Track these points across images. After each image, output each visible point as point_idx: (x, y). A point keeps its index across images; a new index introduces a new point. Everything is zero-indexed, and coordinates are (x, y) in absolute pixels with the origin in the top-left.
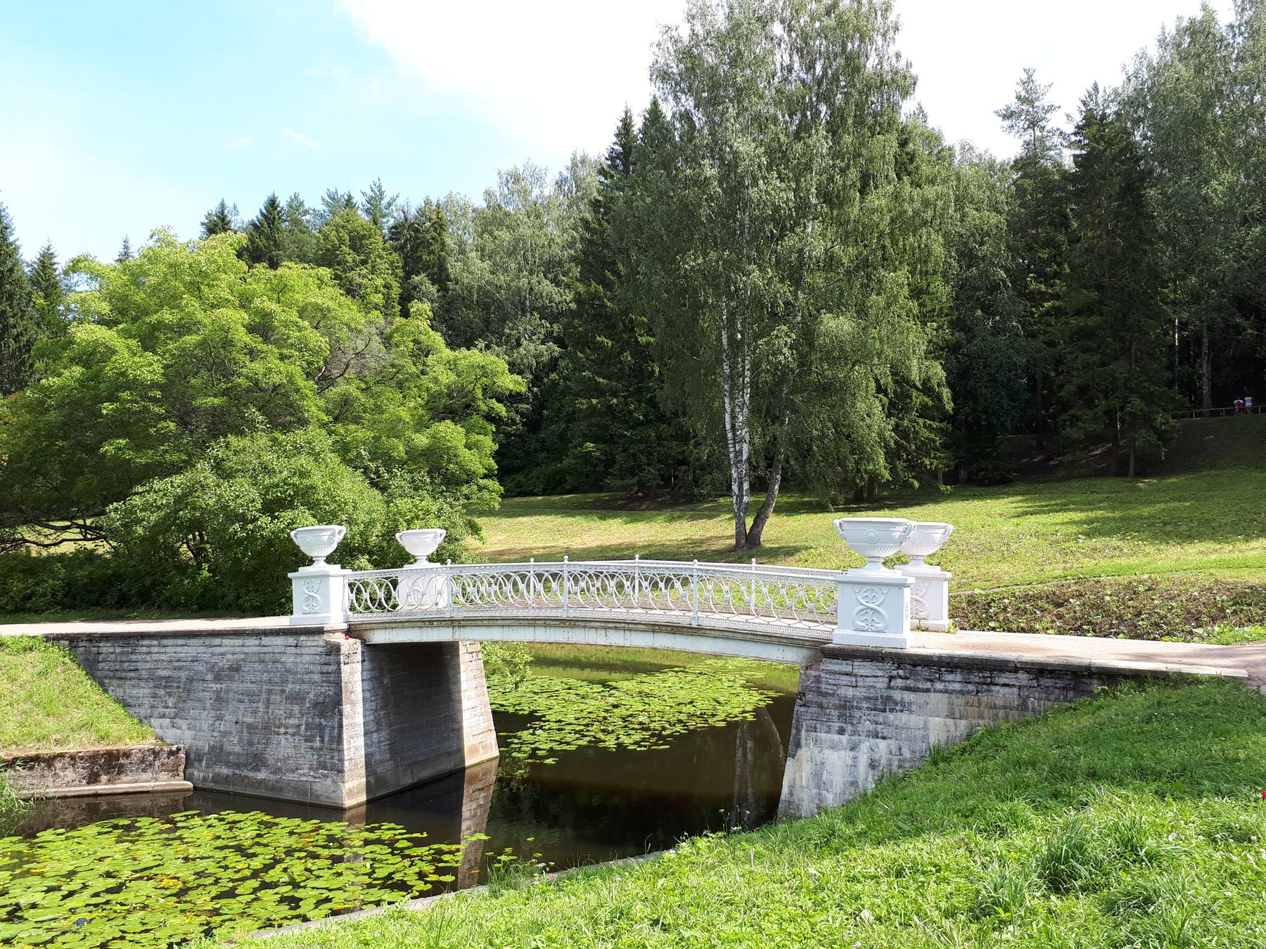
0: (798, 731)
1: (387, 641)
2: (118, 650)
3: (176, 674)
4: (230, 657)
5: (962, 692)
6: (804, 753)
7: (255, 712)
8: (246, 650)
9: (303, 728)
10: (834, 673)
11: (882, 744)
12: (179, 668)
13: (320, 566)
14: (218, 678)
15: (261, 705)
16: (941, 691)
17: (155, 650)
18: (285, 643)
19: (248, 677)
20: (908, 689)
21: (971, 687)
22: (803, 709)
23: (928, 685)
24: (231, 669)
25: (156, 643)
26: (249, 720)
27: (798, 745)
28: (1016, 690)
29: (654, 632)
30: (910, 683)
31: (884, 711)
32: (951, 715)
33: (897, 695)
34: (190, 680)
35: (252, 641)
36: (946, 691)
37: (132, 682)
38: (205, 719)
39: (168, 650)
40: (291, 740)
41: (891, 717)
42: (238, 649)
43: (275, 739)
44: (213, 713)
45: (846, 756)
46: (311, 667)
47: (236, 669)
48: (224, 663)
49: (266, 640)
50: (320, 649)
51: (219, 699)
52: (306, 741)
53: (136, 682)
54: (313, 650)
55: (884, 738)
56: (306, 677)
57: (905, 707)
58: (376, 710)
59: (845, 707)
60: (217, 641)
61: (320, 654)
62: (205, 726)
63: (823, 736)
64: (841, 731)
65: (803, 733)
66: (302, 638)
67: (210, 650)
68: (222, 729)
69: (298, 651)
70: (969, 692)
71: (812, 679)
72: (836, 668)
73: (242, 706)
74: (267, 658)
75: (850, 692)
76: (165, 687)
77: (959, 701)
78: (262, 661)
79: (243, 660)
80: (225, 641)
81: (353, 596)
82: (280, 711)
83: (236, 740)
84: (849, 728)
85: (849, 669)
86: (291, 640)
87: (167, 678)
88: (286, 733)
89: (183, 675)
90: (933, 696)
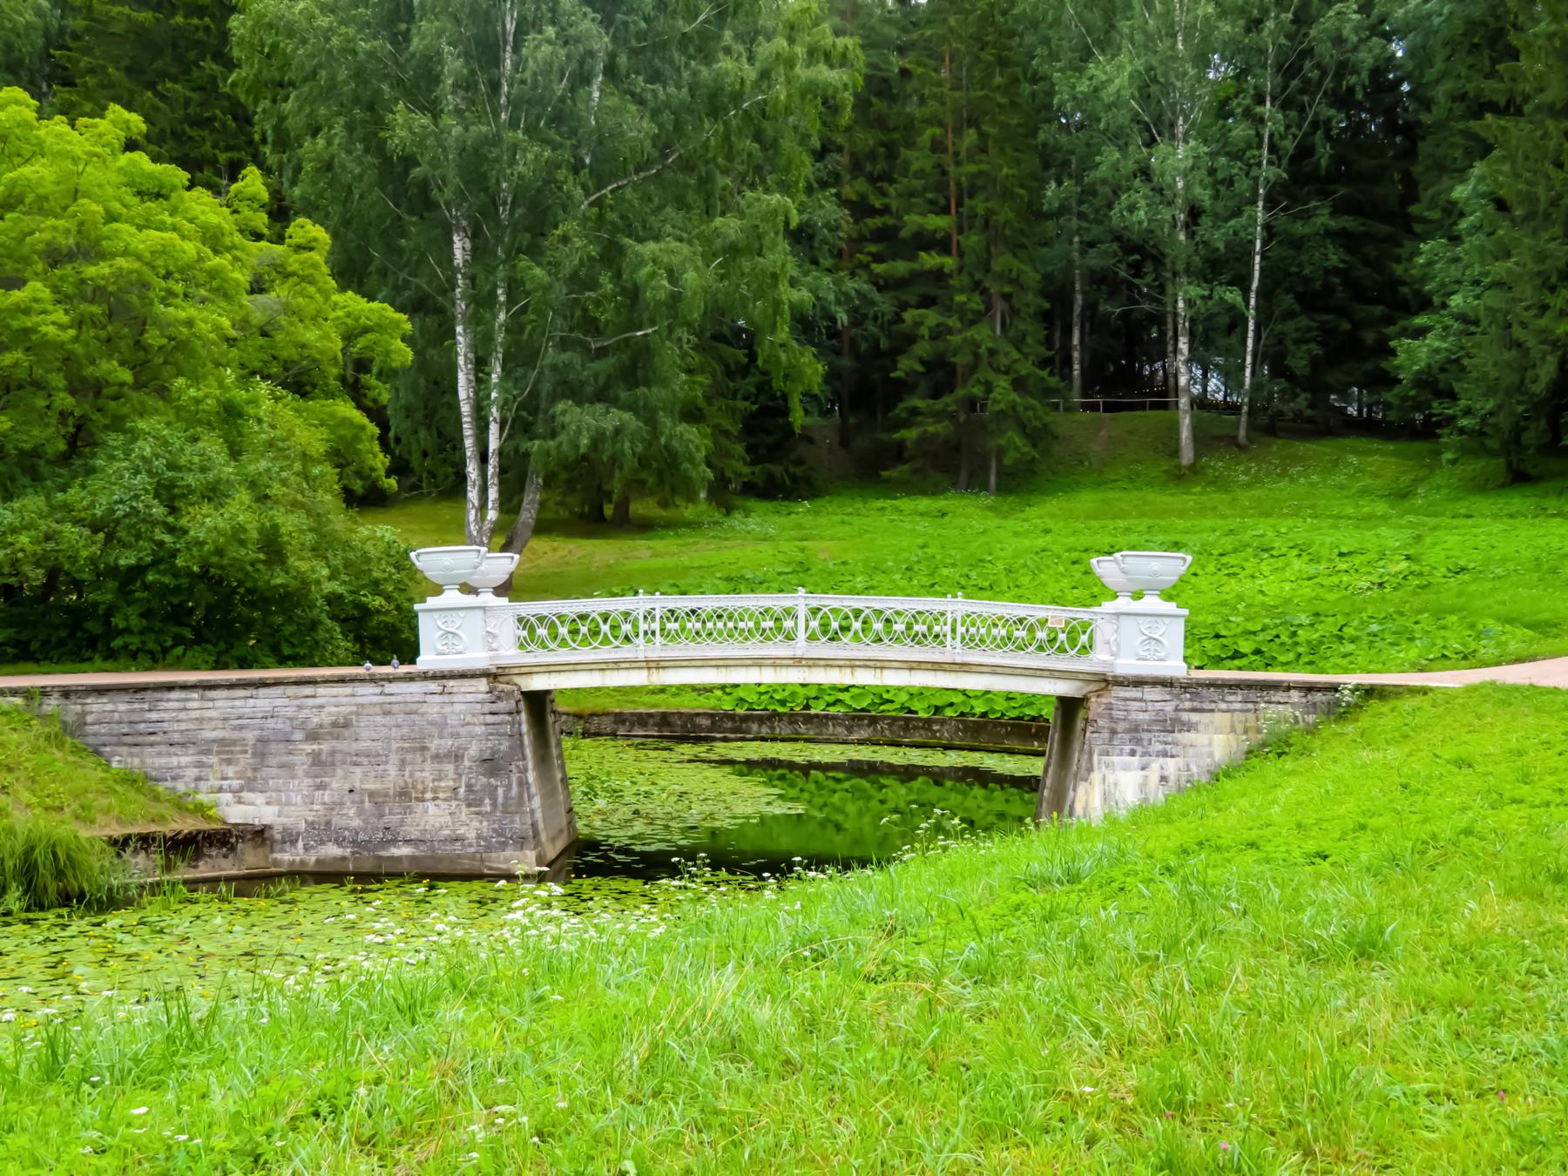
0: (1091, 754)
2: (123, 707)
3: (236, 735)
4: (335, 709)
5: (1242, 711)
6: (1096, 776)
7: (381, 777)
9: (462, 790)
10: (1126, 699)
12: (242, 728)
14: (313, 736)
17: (195, 705)
18: (424, 689)
19: (365, 734)
20: (1194, 710)
21: (1250, 706)
23: (1213, 706)
24: (334, 725)
25: (195, 695)
26: (371, 786)
27: (1090, 769)
29: (911, 669)
30: (1196, 704)
32: (1233, 730)
33: (1185, 716)
34: (263, 741)
35: (370, 689)
37: (156, 749)
38: (300, 786)
39: (219, 704)
40: (444, 805)
41: (1178, 736)
42: (344, 700)
45: (1135, 776)
46: (469, 718)
47: (342, 726)
48: (326, 718)
49: (390, 688)
50: (481, 697)
52: (469, 805)
53: (163, 748)
54: (470, 698)
56: (463, 731)
57: (1190, 727)
59: (1135, 729)
60: (308, 690)
63: (1115, 759)
64: (1133, 753)
65: (1095, 758)
66: (451, 683)
68: (326, 799)
69: (445, 698)
72: (1127, 695)
73: (358, 771)
74: (395, 708)
75: (1142, 716)
76: (219, 753)
77: (1239, 716)
78: (387, 713)
79: (358, 714)
80: (321, 690)
82: (425, 773)
83: (352, 812)
84: (1139, 750)
85: (1139, 695)
86: (433, 686)
87: (221, 742)
88: (434, 799)
89: (251, 736)
90: (1217, 716)
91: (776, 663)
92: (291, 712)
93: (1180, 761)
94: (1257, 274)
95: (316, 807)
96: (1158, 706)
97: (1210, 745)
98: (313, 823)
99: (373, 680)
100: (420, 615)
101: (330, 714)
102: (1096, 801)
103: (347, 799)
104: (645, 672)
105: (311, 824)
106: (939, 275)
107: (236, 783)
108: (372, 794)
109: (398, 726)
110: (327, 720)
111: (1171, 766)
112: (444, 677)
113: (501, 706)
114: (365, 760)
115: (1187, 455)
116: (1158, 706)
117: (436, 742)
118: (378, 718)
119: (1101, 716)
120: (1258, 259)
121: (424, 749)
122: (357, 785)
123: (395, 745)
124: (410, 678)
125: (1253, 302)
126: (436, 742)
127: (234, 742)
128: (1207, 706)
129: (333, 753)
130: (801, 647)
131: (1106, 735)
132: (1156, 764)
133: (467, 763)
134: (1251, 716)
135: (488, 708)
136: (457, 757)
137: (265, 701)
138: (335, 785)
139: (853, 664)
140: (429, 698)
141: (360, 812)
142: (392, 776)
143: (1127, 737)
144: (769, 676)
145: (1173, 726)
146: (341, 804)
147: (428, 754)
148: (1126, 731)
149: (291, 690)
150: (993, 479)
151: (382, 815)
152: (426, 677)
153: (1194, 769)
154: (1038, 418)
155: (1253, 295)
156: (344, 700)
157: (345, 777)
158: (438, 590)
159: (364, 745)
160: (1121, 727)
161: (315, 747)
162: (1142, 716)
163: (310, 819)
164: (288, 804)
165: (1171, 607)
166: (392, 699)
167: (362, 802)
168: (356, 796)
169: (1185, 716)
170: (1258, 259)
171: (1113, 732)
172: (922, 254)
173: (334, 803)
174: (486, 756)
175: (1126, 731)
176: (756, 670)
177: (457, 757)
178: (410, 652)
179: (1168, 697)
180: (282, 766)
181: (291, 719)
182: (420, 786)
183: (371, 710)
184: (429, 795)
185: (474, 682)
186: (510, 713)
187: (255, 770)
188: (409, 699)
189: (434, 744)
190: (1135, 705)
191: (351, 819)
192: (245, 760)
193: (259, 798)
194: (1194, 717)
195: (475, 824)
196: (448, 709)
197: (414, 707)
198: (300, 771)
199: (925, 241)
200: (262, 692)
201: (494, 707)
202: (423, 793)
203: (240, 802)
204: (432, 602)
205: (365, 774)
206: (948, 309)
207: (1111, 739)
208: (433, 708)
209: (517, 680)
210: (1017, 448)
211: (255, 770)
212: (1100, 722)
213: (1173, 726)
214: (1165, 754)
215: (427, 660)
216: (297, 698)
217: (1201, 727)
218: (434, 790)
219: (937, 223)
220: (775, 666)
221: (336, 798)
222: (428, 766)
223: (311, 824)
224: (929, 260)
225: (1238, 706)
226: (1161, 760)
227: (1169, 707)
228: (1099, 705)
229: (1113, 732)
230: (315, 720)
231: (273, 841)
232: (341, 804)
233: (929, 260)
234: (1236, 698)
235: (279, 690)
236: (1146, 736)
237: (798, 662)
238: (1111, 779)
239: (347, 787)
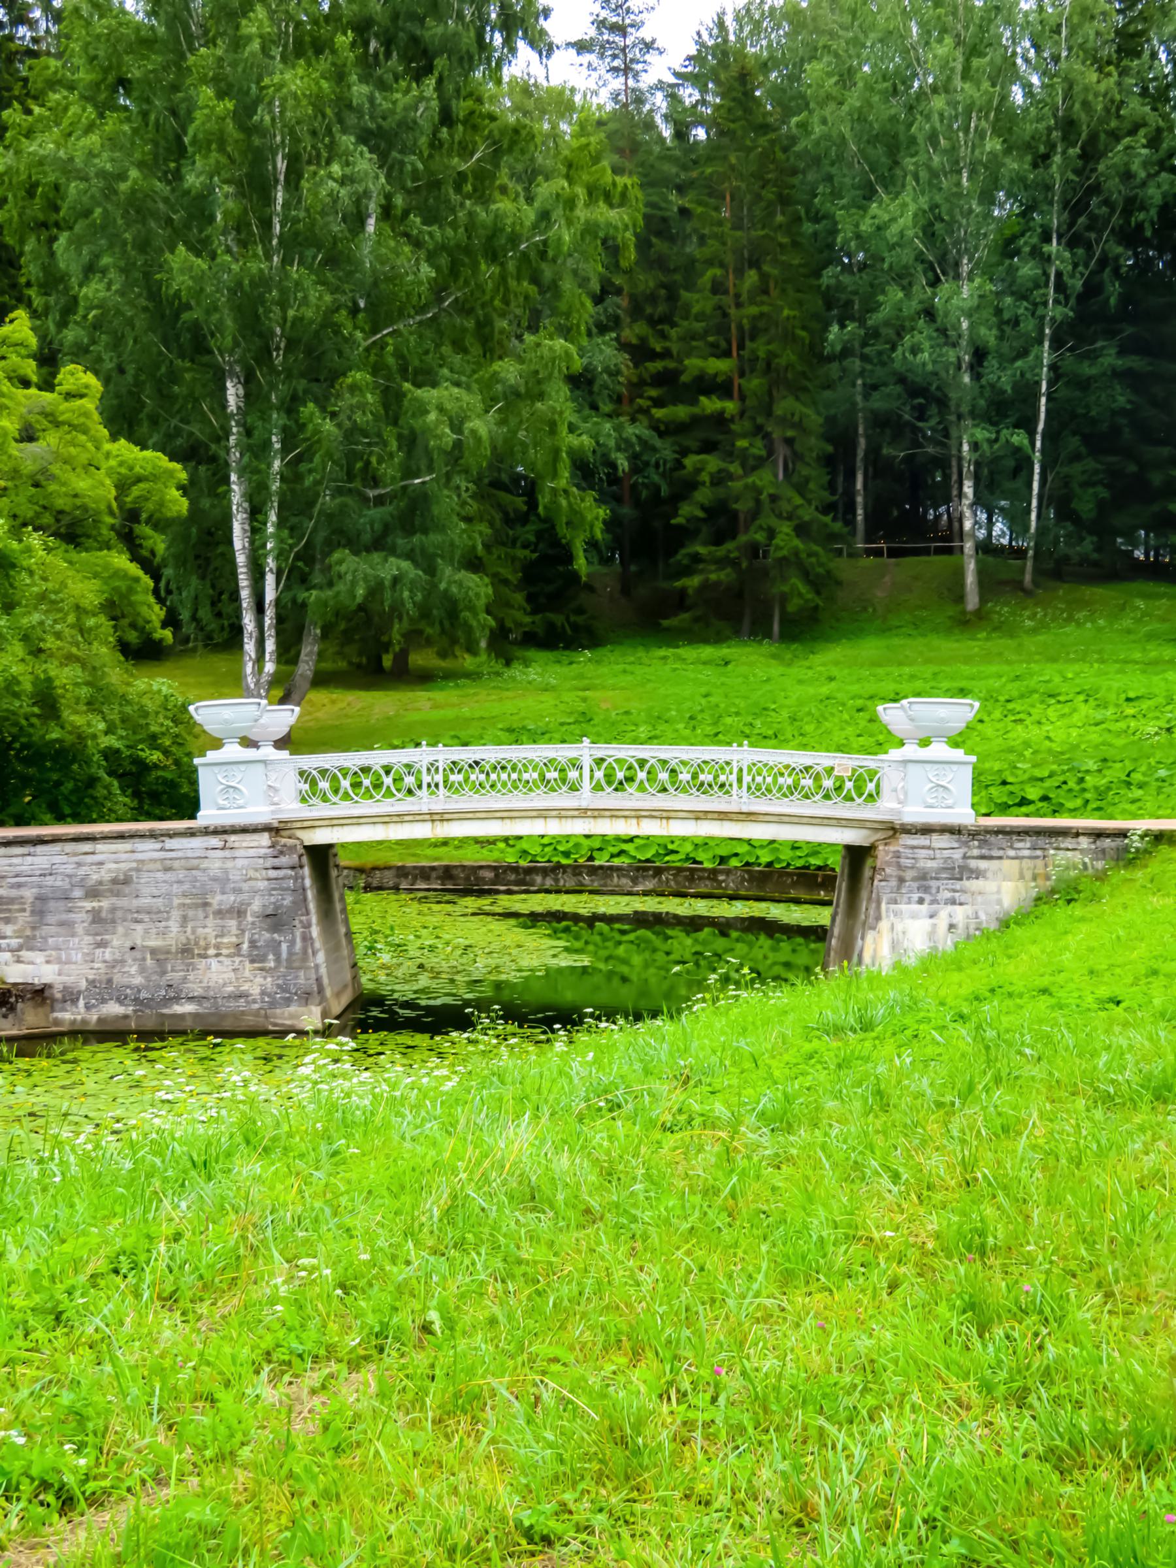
3: (14, 893)
6: (884, 925)
7: (163, 934)
8: (139, 856)
9: (245, 946)
12: (19, 886)
14: (93, 893)
19: (146, 891)
20: (983, 857)
24: (115, 881)
26: (153, 943)
27: (878, 918)
30: (984, 851)
33: (973, 863)
34: (40, 898)
38: (81, 942)
40: (227, 961)
41: (966, 884)
42: (124, 856)
43: (202, 964)
45: (926, 923)
46: (251, 873)
47: (122, 882)
48: (105, 874)
49: (171, 843)
50: (263, 851)
51: (96, 917)
54: (252, 852)
57: (978, 874)
59: (923, 877)
60: (87, 847)
61: (264, 857)
63: (903, 907)
64: (921, 901)
65: (883, 906)
66: (233, 838)
68: (108, 956)
69: (227, 853)
74: (176, 864)
77: (1027, 863)
78: (167, 869)
79: (138, 870)
80: (100, 847)
82: (208, 930)
83: (133, 970)
84: (928, 898)
86: (215, 841)
89: (29, 894)
90: (1006, 863)
91: (561, 814)
92: (70, 868)
94: (1042, 416)
96: (946, 853)
99: (153, 835)
100: (202, 772)
102: (885, 950)
103: (129, 957)
105: (92, 983)
106: (720, 420)
107: (14, 942)
108: (153, 951)
109: (179, 882)
110: (107, 877)
111: (960, 914)
112: (225, 832)
113: (284, 860)
114: (146, 917)
115: (972, 601)
116: (946, 853)
117: (219, 897)
118: (159, 875)
119: (889, 864)
120: (1043, 400)
121: (206, 905)
122: (139, 942)
123: (176, 902)
124: (191, 833)
125: (1038, 444)
126: (219, 897)
127: (12, 901)
128: (995, 853)
129: (113, 910)
130: (586, 798)
131: (894, 883)
132: (944, 912)
133: (250, 919)
134: (1040, 863)
135: (270, 862)
137: (43, 858)
138: (115, 943)
139: (639, 815)
140: (211, 853)
141: (142, 970)
142: (174, 934)
143: (915, 885)
144: (554, 828)
146: (123, 962)
147: (210, 910)
148: (914, 879)
149: (70, 847)
150: (776, 627)
151: (164, 973)
152: (207, 832)
153: (983, 917)
154: (821, 565)
155: (1038, 438)
156: (124, 856)
157: (126, 935)
158: (217, 744)
160: (909, 875)
164: (69, 962)
165: (958, 754)
168: (137, 954)
169: (973, 863)
170: (1043, 400)
171: (901, 880)
172: (703, 399)
175: (914, 879)
176: (541, 822)
177: (239, 912)
178: (188, 806)
180: (61, 924)
183: (151, 866)
184: (212, 952)
185: (255, 836)
187: (34, 928)
188: (190, 854)
189: (216, 900)
192: (24, 918)
193: (38, 957)
194: (983, 864)
195: (259, 980)
196: (229, 864)
198: (79, 928)
199: (707, 385)
200: (40, 849)
203: (19, 961)
204: (212, 756)
205: (146, 931)
206: (730, 455)
208: (215, 864)
209: (299, 834)
210: (800, 595)
211: (34, 928)
212: (888, 871)
214: (953, 902)
215: (207, 815)
218: (217, 947)
219: (718, 366)
221: (118, 956)
224: (710, 404)
225: (1027, 853)
226: (950, 908)
227: (957, 855)
229: (901, 880)
230: (95, 877)
231: (53, 1000)
232: (123, 962)
233: (710, 404)
235: (57, 847)
236: (934, 884)
237: (584, 813)
238: (899, 927)
239: (129, 944)
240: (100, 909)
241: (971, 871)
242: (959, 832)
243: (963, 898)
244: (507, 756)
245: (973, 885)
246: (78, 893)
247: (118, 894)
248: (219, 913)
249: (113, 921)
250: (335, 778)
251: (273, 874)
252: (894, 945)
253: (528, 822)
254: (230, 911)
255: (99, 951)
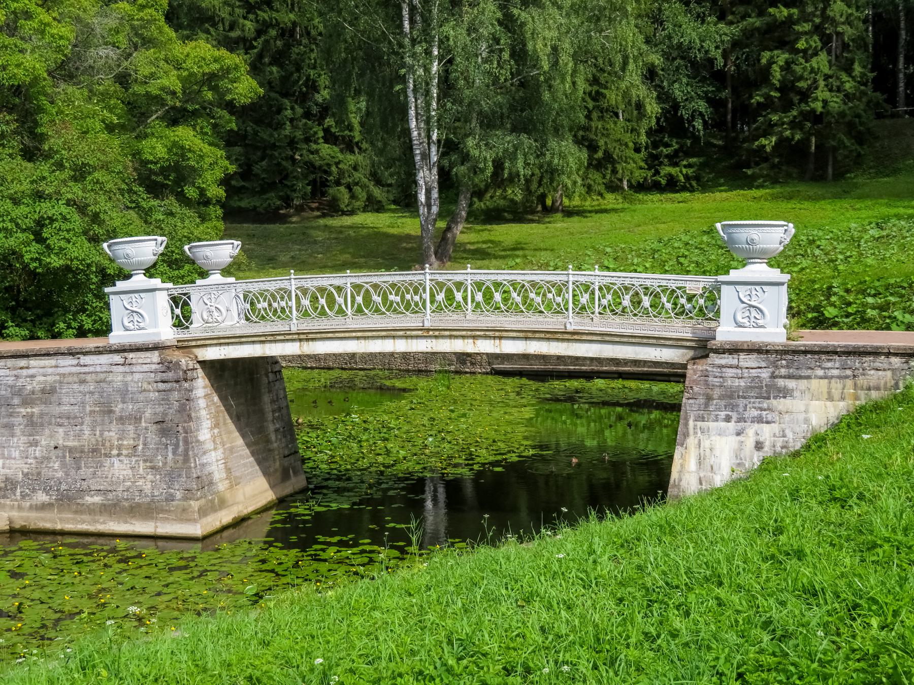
1: (222, 357)
4: (43, 378)
5: (840, 377)
6: (691, 441)
7: (78, 436)
8: (61, 370)
10: (721, 367)
11: (765, 427)
13: (139, 280)
14: (26, 403)
15: (85, 427)
16: (821, 378)
18: (110, 361)
19: (65, 400)
20: (790, 377)
21: (849, 372)
22: (691, 401)
23: (809, 372)
24: (43, 391)
26: (70, 444)
27: (686, 435)
28: (889, 373)
29: (526, 338)
31: (769, 398)
32: (830, 398)
33: (781, 382)
35: (70, 361)
36: (825, 377)
41: (774, 402)
42: (50, 371)
44: (24, 439)
46: (145, 386)
47: (48, 393)
49: (85, 360)
50: (154, 367)
54: (145, 368)
55: (768, 422)
56: (141, 397)
57: (785, 393)
58: (212, 429)
59: (731, 397)
60: (23, 362)
61: (155, 372)
62: (16, 454)
63: (711, 425)
64: (728, 419)
66: (131, 355)
67: (15, 372)
68: (38, 454)
69: (127, 369)
70: (847, 377)
71: (699, 373)
72: (723, 362)
73: (61, 430)
74: (88, 378)
75: (737, 383)
78: (83, 382)
80: (33, 362)
81: (178, 311)
84: (734, 416)
85: (735, 362)
86: (117, 358)
88: (119, 455)
90: (814, 383)
91: (407, 334)
92: (10, 381)
93: (775, 427)
95: (30, 461)
97: (806, 412)
98: (27, 474)
99: (71, 353)
100: (114, 301)
101: (39, 383)
102: (692, 465)
104: (298, 344)
105: (26, 475)
108: (71, 450)
109: (91, 393)
110: (37, 388)
111: (767, 432)
112: (124, 351)
113: (170, 375)
114: (66, 422)
117: (120, 406)
118: (76, 386)
122: (61, 442)
123: (88, 409)
124: (98, 352)
126: (120, 406)
129: (42, 415)
131: (701, 400)
132: (751, 430)
133: (143, 424)
134: (849, 383)
135: (160, 376)
136: (136, 419)
138: (43, 443)
139: (474, 335)
141: (63, 465)
143: (723, 403)
144: (401, 346)
145: (768, 392)
146: (48, 459)
149: (10, 362)
150: (830, 171)
151: (79, 468)
153: (790, 435)
154: (861, 124)
156: (50, 371)
157: (51, 436)
159: (65, 408)
160: (717, 393)
161: (29, 410)
162: (737, 383)
163: (26, 471)
164: (10, 458)
166: (86, 369)
167: (64, 457)
169: (781, 382)
172: (771, 10)
173: (43, 457)
174: (159, 419)
176: (391, 341)
177: (136, 419)
178: (104, 330)
179: (763, 364)
181: (11, 387)
182: (108, 444)
183: (70, 379)
184: (115, 452)
185: (148, 354)
186: (177, 382)
188: (98, 369)
189: (118, 408)
190: (731, 372)
191: (56, 471)
194: (791, 384)
195: (150, 477)
196: (129, 378)
197: (102, 376)
198: (17, 430)
201: (165, 376)
202: (111, 448)
204: (121, 285)
205: (66, 434)
207: (707, 405)
208: (117, 378)
210: (845, 147)
212: (696, 389)
213: (768, 392)
214: (760, 420)
215: (117, 336)
216: (15, 369)
217: (795, 394)
218: (119, 448)
220: (407, 337)
221: (45, 453)
222: (114, 427)
223: (26, 475)
225: (836, 372)
227: (765, 374)
228: (695, 371)
229: (709, 398)
230: (29, 388)
234: (833, 366)
236: (741, 402)
237: (426, 333)
238: (706, 443)
239: (53, 444)
240: (32, 415)
241: (779, 390)
242: (767, 352)
243: (770, 418)
244: (263, 286)
245: (780, 404)
246: (16, 401)
247: (46, 403)
248: (121, 420)
249: (42, 425)
250: (367, 294)
251: (161, 386)
252: (700, 461)
253: (379, 342)
254: (130, 417)
255: (31, 449)
